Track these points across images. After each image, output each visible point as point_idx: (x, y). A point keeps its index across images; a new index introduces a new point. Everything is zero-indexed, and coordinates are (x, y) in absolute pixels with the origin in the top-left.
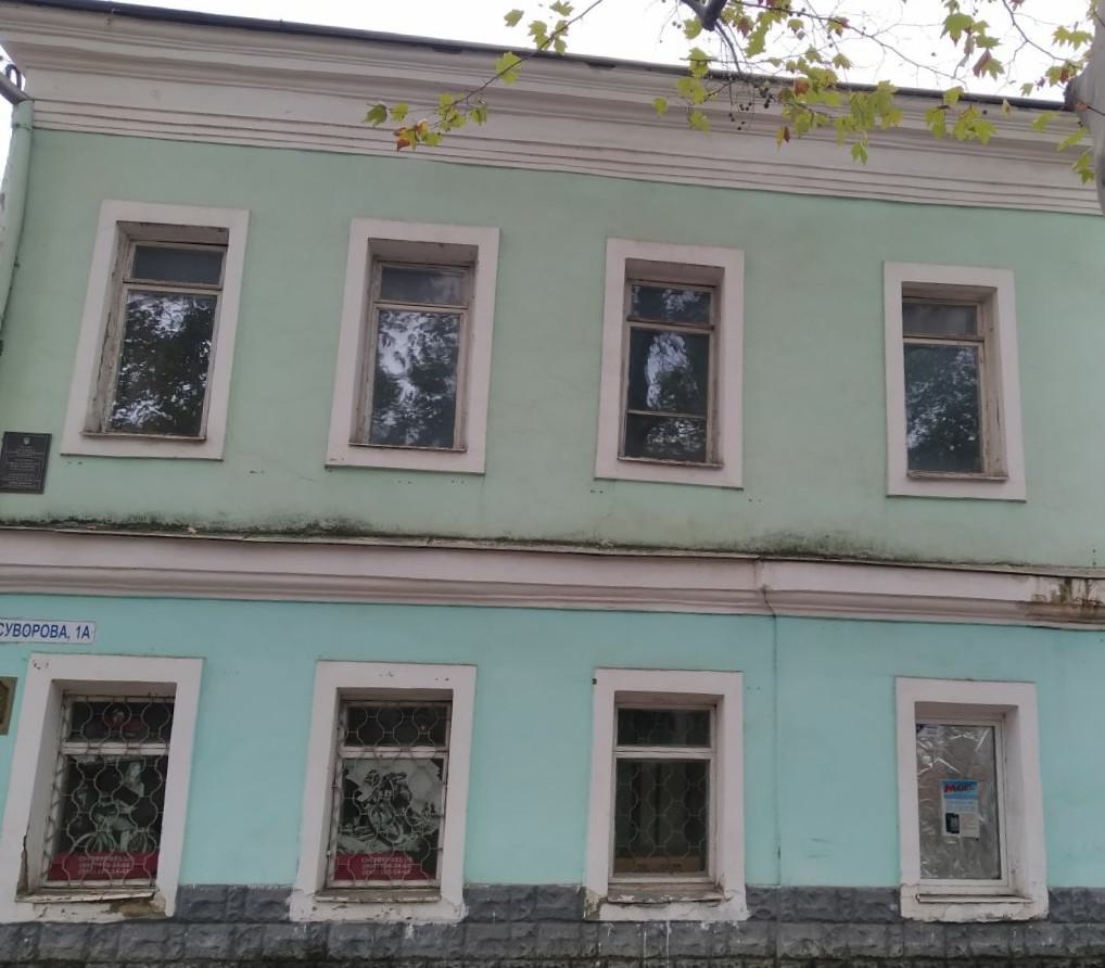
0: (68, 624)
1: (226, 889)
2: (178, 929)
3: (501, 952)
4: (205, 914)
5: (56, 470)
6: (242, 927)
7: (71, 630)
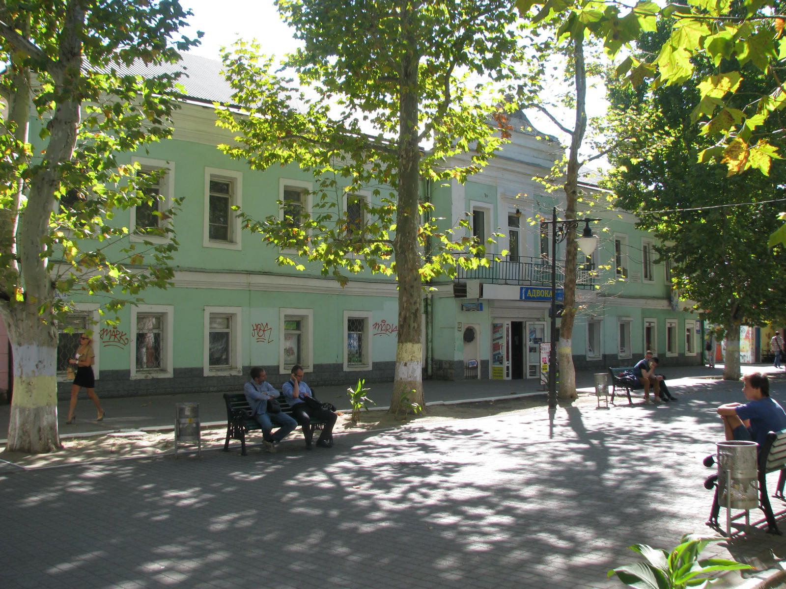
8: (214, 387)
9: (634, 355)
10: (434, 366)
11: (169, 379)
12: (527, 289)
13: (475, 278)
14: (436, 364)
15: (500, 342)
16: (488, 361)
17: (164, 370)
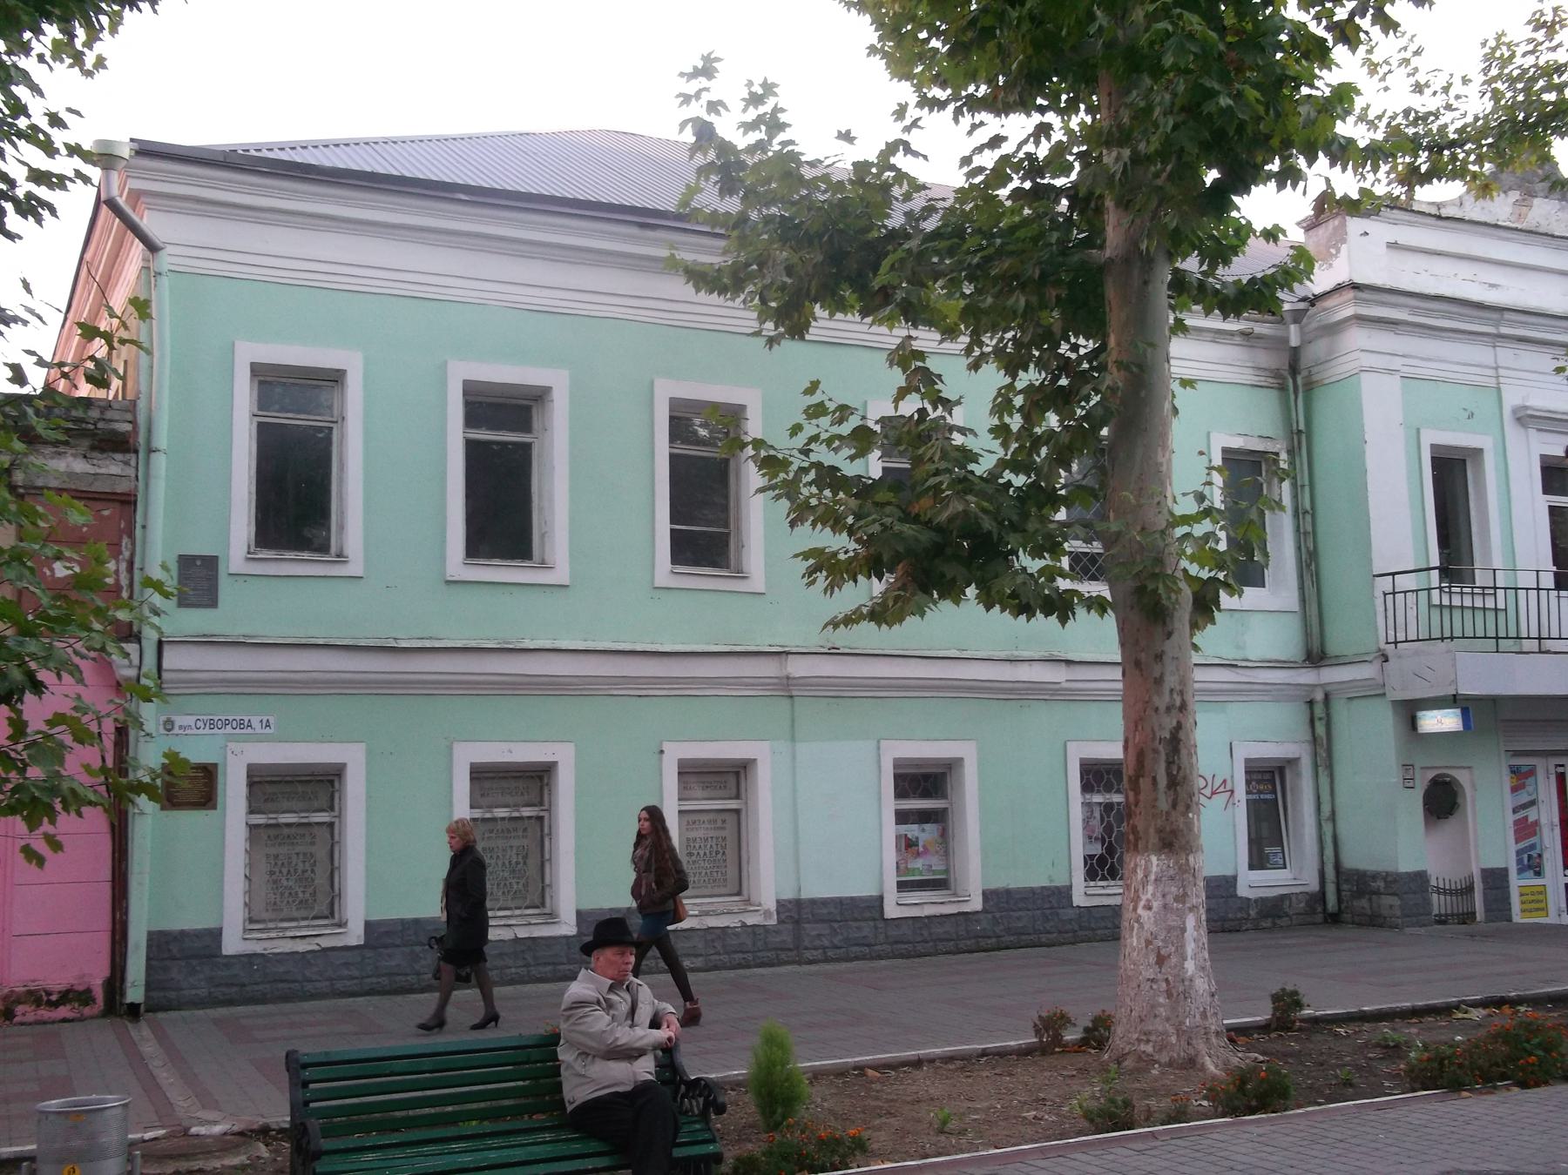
0: (252, 718)
2: (369, 953)
5: (226, 589)
7: (255, 722)
8: (696, 956)
10: (1345, 887)
11: (566, 937)
13: (1442, 639)
14: (1347, 881)
15: (1532, 814)
16: (1506, 870)
17: (552, 917)
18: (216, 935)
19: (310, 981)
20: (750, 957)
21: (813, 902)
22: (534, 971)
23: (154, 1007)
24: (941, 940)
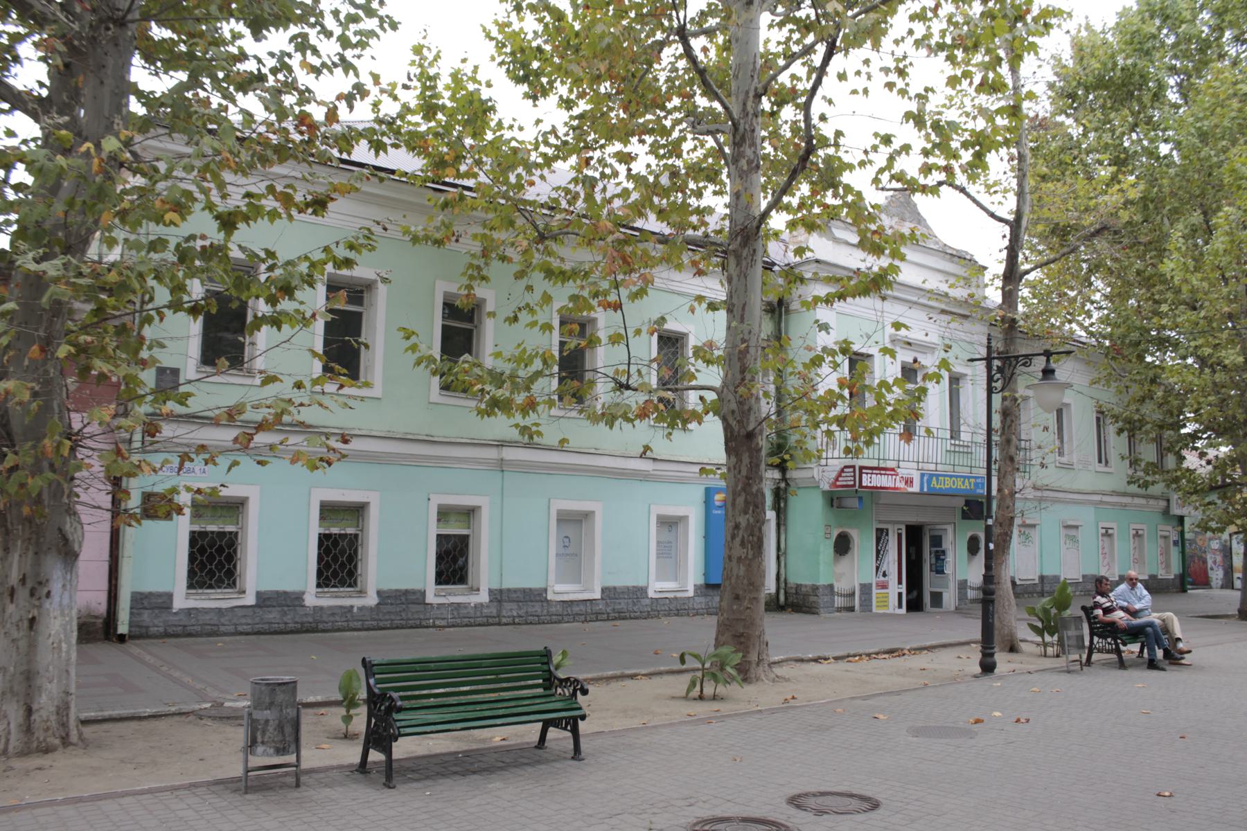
1: (277, 592)
2: (257, 610)
3: (393, 617)
4: (269, 603)
6: (286, 608)
9: (1084, 577)
12: (931, 476)
17: (362, 593)
18: (170, 596)
19: (223, 625)
20: (472, 620)
21: (509, 590)
22: (352, 625)
23: (132, 636)
24: (577, 614)
